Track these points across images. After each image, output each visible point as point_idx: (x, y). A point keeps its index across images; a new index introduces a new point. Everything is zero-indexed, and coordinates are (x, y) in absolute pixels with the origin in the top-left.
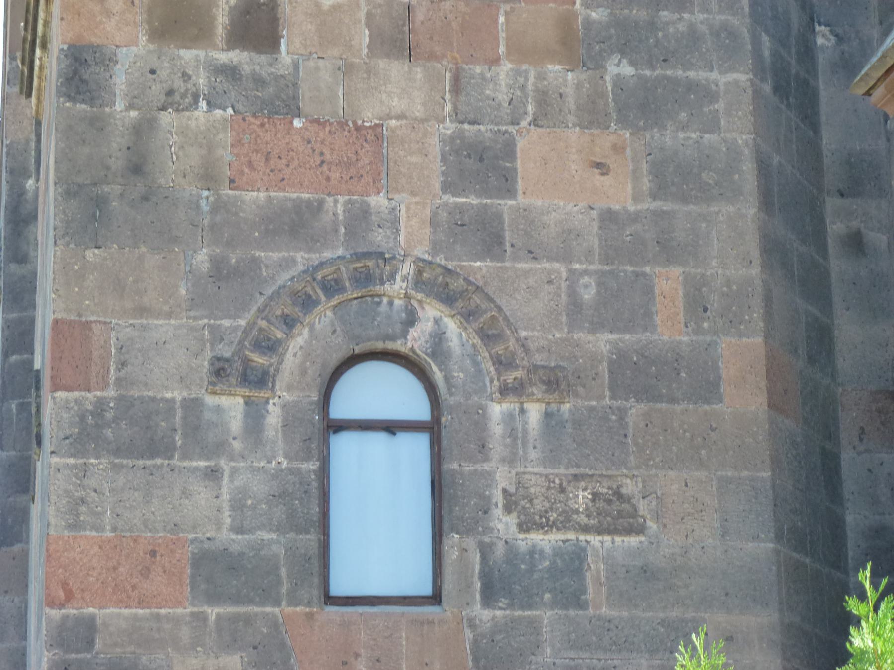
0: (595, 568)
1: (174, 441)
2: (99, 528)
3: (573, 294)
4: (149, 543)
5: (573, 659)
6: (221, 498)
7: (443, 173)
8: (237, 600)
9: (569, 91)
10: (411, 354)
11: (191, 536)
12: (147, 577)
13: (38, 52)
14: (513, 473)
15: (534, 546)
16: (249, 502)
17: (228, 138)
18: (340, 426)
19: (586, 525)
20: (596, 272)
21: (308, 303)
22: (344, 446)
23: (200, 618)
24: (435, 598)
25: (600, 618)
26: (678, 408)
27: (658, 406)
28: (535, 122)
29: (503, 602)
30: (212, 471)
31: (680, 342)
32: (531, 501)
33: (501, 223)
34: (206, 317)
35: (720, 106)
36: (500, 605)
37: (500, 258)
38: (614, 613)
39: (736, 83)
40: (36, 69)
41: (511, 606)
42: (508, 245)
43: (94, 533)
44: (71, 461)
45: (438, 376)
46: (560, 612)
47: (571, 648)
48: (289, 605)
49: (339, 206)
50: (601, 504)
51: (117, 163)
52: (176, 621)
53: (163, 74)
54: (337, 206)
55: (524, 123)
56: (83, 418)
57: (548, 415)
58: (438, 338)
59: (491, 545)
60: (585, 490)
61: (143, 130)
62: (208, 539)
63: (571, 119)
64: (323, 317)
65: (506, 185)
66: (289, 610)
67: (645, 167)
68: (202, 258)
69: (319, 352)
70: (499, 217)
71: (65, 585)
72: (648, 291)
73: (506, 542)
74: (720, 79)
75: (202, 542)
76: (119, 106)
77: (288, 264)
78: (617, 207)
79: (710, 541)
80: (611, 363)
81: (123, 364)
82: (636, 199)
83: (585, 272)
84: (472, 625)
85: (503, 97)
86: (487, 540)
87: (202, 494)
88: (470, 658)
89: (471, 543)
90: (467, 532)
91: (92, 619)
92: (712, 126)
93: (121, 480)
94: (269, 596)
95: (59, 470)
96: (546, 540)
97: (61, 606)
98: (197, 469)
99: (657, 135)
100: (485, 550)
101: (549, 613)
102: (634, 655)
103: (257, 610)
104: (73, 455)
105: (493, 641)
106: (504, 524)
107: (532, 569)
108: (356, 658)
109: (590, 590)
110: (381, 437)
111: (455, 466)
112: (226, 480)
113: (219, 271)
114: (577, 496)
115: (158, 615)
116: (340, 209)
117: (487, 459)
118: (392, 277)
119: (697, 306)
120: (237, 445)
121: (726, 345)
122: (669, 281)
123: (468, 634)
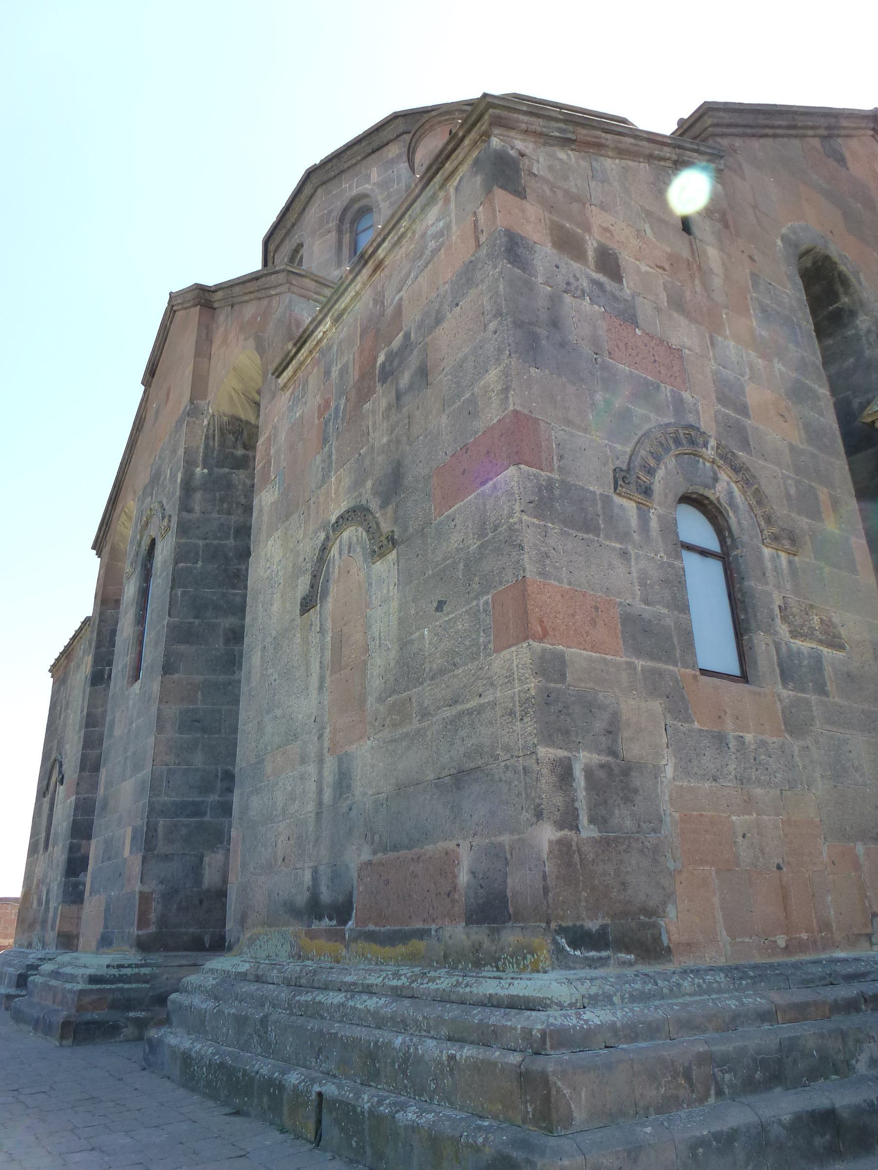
0: (828, 671)
2: (560, 580)
3: (786, 488)
8: (652, 657)
23: (631, 666)
24: (744, 678)
44: (535, 521)
45: (733, 520)
53: (564, 270)
56: (540, 490)
61: (555, 300)
76: (540, 280)
78: (794, 443)
84: (780, 700)
103: (665, 667)
104: (535, 517)
106: (783, 629)
109: (828, 684)
111: (752, 583)
115: (605, 659)
120: (636, 536)
121: (853, 539)
123: (779, 706)
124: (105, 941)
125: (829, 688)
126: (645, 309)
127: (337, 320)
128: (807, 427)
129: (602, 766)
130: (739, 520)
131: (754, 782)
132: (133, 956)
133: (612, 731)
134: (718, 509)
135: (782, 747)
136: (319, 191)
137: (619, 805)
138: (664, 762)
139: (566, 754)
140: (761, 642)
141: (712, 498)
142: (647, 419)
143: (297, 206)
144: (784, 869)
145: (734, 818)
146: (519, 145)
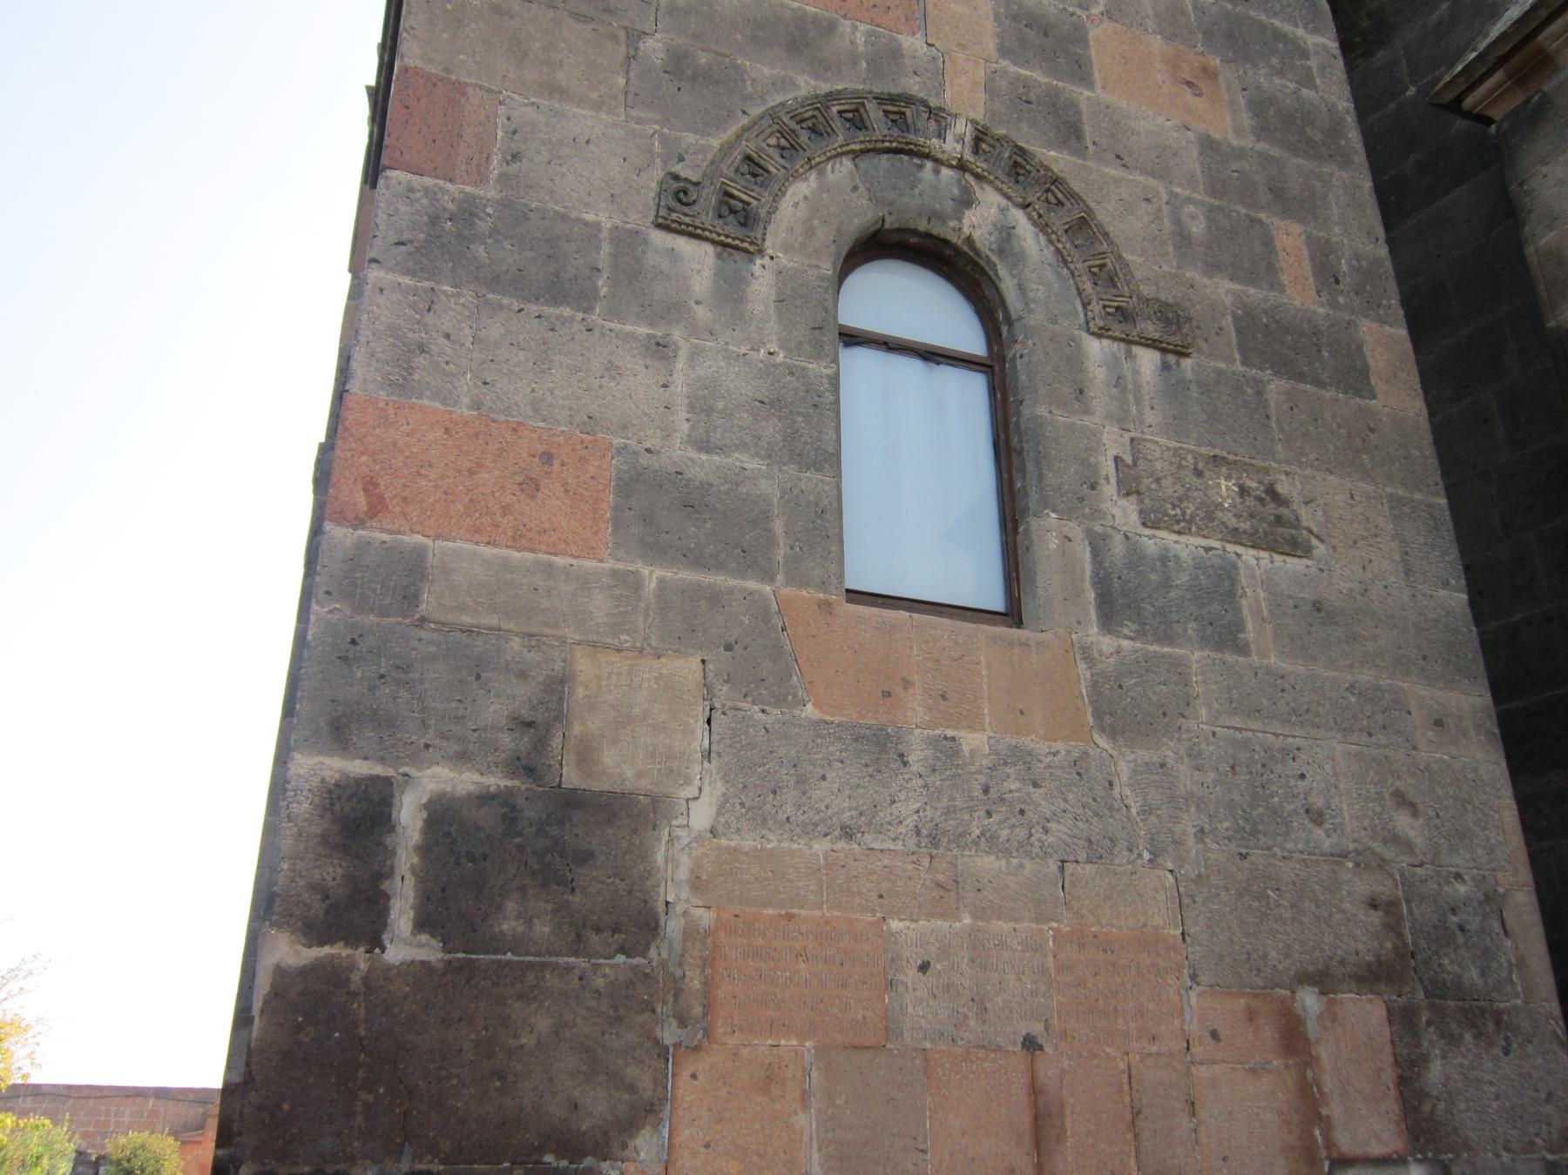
0: (1252, 600)
1: (595, 288)
3: (1177, 222)
4: (540, 439)
5: (1240, 730)
6: (672, 388)
7: (998, 34)
8: (697, 561)
10: (965, 248)
11: (617, 441)
12: (533, 497)
14: (1127, 436)
15: (1166, 549)
16: (720, 405)
18: (852, 338)
19: (1236, 529)
20: (1203, 203)
22: (859, 366)
23: (633, 583)
24: (1013, 614)
25: (1269, 671)
26: (1329, 394)
27: (1302, 386)
29: (1130, 628)
30: (658, 344)
31: (1314, 312)
32: (1158, 480)
33: (1078, 112)
34: (657, 122)
35: (1313, 63)
36: (1126, 631)
37: (1081, 152)
38: (1284, 666)
39: (1325, 47)
41: (1140, 635)
42: (1089, 143)
43: (437, 405)
44: (407, 281)
45: (1008, 284)
46: (1212, 655)
47: (1235, 712)
48: (787, 583)
49: (858, 34)
50: (1250, 502)
52: (584, 582)
55: (1095, 11)
56: (435, 220)
57: (1165, 367)
59: (1105, 537)
60: (1228, 478)
62: (648, 451)
63: (1151, 25)
65: (1080, 71)
66: (787, 591)
67: (1242, 102)
68: (654, 47)
69: (832, 209)
70: (1073, 105)
71: (370, 485)
72: (1268, 243)
73: (1127, 537)
75: (636, 453)
78: (1216, 136)
79: (1393, 579)
80: (1237, 320)
81: (516, 157)
82: (1238, 131)
83: (1189, 200)
84: (1088, 658)
86: (1098, 529)
88: (1089, 710)
89: (1075, 530)
90: (1068, 514)
91: (420, 553)
92: (1307, 80)
93: (494, 330)
94: (753, 560)
95: (381, 290)
96: (1186, 546)
97: (359, 523)
98: (632, 336)
99: (1250, 73)
100: (1098, 545)
101: (1197, 655)
102: (1322, 733)
104: (407, 272)
105: (1120, 687)
106: (1123, 513)
107: (1166, 584)
108: (905, 688)
109: (1250, 626)
110: (914, 365)
111: (1042, 411)
112: (680, 364)
114: (1219, 485)
115: (550, 564)
116: (860, 39)
117: (1087, 412)
118: (941, 135)
120: (701, 313)
121: (1367, 329)
122: (1290, 238)
125: (1250, 633)
128: (1260, 106)
129: (485, 798)
131: (976, 843)
134: (976, 264)
135: (1078, 766)
137: (523, 890)
138: (691, 791)
139: (378, 770)
140: (1050, 533)
141: (954, 239)
144: (1048, 1049)
145: (895, 925)
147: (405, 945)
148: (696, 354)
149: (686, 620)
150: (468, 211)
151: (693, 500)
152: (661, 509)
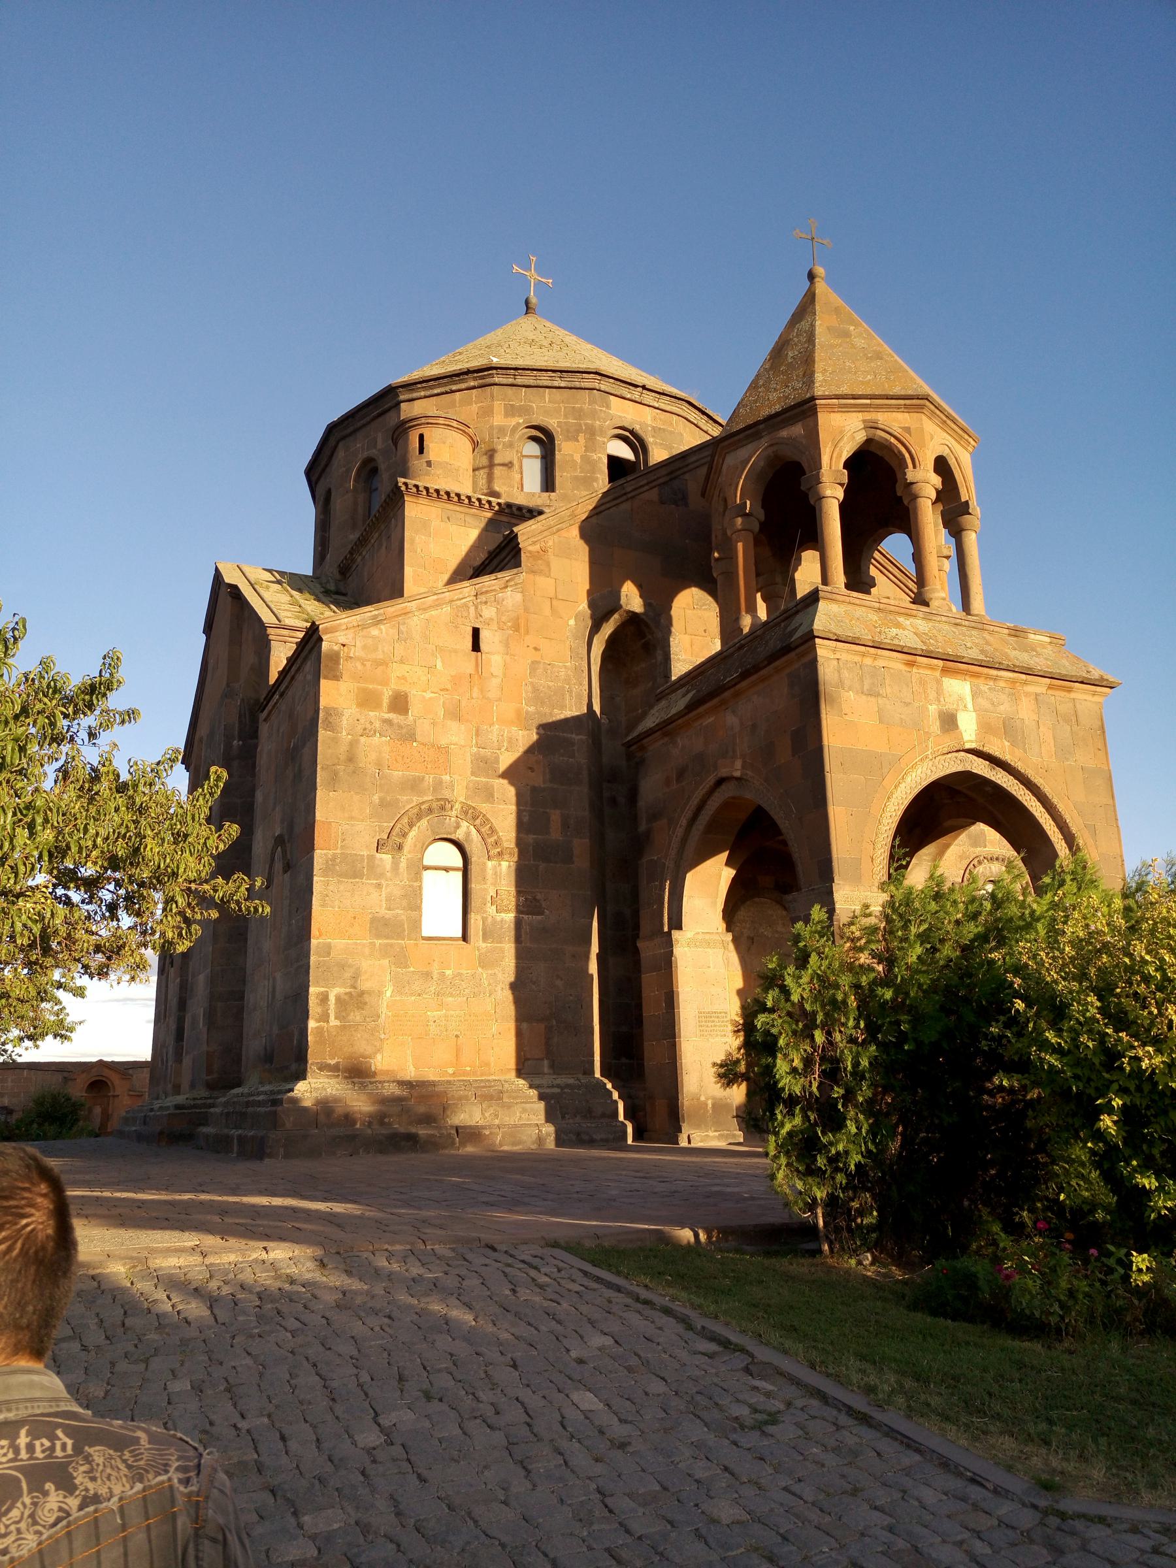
9: (520, 738)
13: (277, 697)
17: (387, 749)
18: (427, 868)
21: (419, 817)
22: (427, 875)
28: (507, 750)
40: (271, 703)
51: (342, 757)
52: (364, 945)
53: (362, 721)
54: (429, 779)
58: (468, 834)
61: (353, 744)
64: (424, 823)
68: (376, 798)
70: (492, 786)
71: (319, 930)
74: (575, 737)
76: (344, 733)
77: (408, 801)
85: (495, 739)
87: (375, 895)
89: (479, 917)
93: (342, 888)
100: (484, 920)
106: (492, 910)
107: (502, 928)
113: (383, 804)
119: (565, 825)
120: (388, 874)
124: (193, 1086)
126: (424, 729)
127: (281, 695)
130: (475, 847)
132: (204, 1093)
133: (355, 977)
136: (341, 445)
140: (473, 918)
142: (408, 802)
143: (327, 452)
146: (342, 640)
147: (333, 1022)
148: (387, 885)
149: (385, 952)
150: (334, 859)
151: (386, 922)
152: (382, 927)
